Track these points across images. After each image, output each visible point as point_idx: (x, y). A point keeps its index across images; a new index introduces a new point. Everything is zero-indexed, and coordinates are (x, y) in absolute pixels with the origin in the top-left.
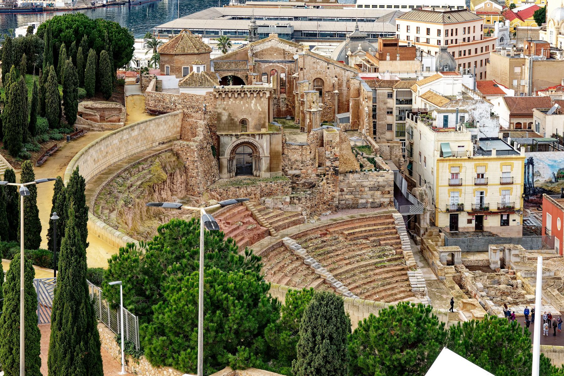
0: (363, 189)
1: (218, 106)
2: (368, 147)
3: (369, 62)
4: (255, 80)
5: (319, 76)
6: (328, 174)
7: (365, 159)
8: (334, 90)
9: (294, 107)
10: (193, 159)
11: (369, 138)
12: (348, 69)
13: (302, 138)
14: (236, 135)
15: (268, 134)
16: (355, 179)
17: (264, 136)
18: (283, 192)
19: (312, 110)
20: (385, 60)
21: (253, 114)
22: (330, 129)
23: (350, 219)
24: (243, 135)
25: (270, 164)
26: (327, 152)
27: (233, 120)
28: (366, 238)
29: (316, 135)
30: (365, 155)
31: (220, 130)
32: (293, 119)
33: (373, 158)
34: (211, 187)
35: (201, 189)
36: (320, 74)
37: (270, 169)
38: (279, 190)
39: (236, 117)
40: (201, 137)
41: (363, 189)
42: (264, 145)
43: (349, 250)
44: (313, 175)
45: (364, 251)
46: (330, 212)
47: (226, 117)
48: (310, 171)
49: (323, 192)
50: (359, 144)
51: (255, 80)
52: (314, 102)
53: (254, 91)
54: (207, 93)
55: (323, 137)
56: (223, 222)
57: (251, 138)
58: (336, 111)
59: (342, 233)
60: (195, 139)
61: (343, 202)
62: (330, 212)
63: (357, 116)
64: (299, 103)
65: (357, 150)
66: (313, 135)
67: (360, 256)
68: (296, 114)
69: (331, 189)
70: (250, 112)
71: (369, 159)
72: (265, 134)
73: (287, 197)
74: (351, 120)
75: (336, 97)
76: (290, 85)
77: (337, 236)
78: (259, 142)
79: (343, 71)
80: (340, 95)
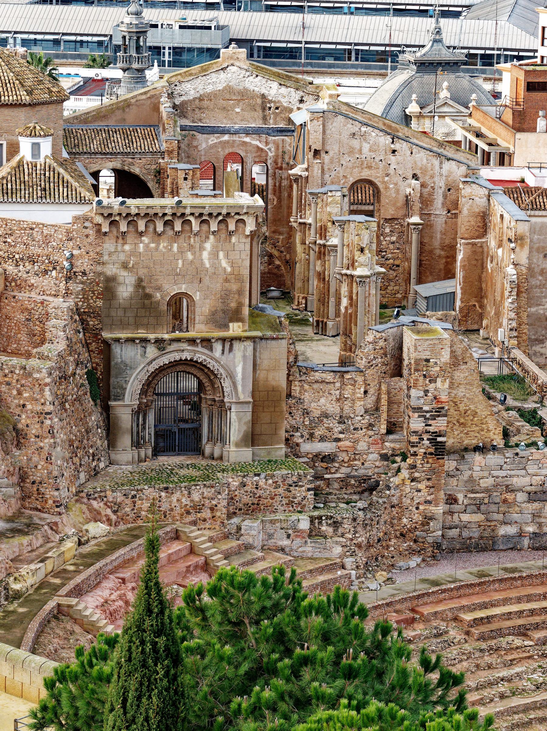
0: (510, 497)
1: (106, 258)
2: (516, 380)
3: (479, 135)
4: (189, 182)
5: (366, 174)
6: (415, 454)
7: (513, 413)
8: (408, 215)
9: (290, 264)
10: (39, 408)
11: (518, 354)
12: (450, 155)
13: (324, 352)
14: (159, 342)
15: (248, 338)
16: (488, 468)
17: (237, 345)
18: (290, 503)
19: (359, 272)
20: (533, 130)
21: (206, 280)
22: (420, 326)
23: (477, 581)
24: (178, 340)
25: (254, 421)
26: (414, 393)
27: (148, 296)
28: (523, 632)
29: (381, 343)
30: (510, 402)
31: (111, 328)
32: (286, 296)
33: (535, 411)
34: (89, 488)
35: (64, 493)
36: (370, 167)
37: (252, 438)
38: (278, 498)
39: (159, 288)
40: (61, 346)
41: (510, 497)
42: (236, 368)
43: (477, 666)
44: (371, 457)
45: (518, 669)
46: (419, 560)
47: (131, 289)
48: (362, 446)
49: (399, 505)
50: (490, 370)
51: (189, 182)
52: (362, 250)
53: (210, 215)
54: (76, 219)
55: (400, 348)
56: (130, 585)
57: (200, 349)
58: (413, 275)
59: (456, 619)
60: (45, 349)
61: (454, 533)
62: (419, 560)
63: (478, 289)
64: (308, 250)
65: (487, 388)
66: (375, 342)
67: (509, 680)
68: (298, 284)
69: (424, 495)
70: (198, 275)
71: (522, 412)
72: (239, 339)
73: (301, 517)
74: (458, 303)
75: (414, 237)
76: (280, 199)
77: (443, 626)
78: (224, 360)
79: (436, 162)
80: (425, 229)
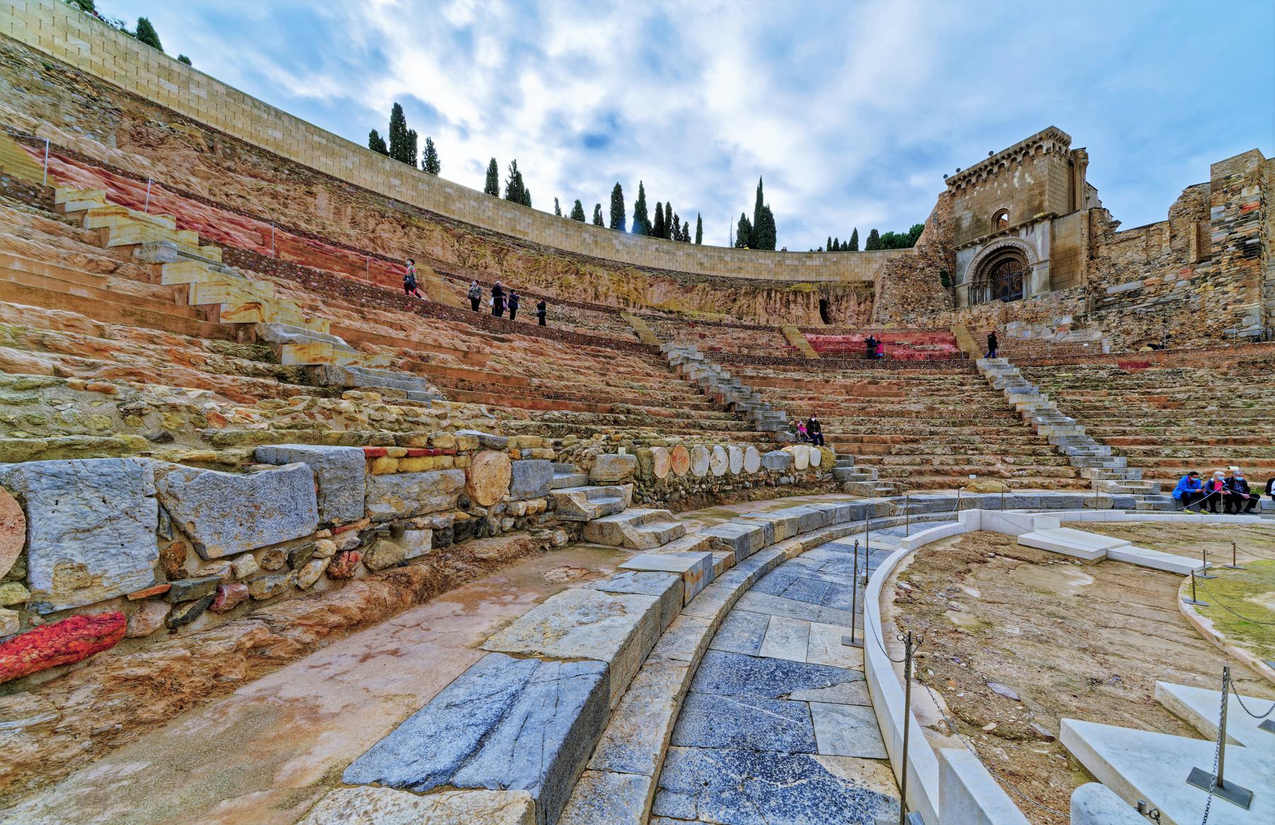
21: (1017, 196)
27: (979, 220)
44: (1179, 284)
49: (1202, 309)
53: (1016, 152)
70: (1011, 195)
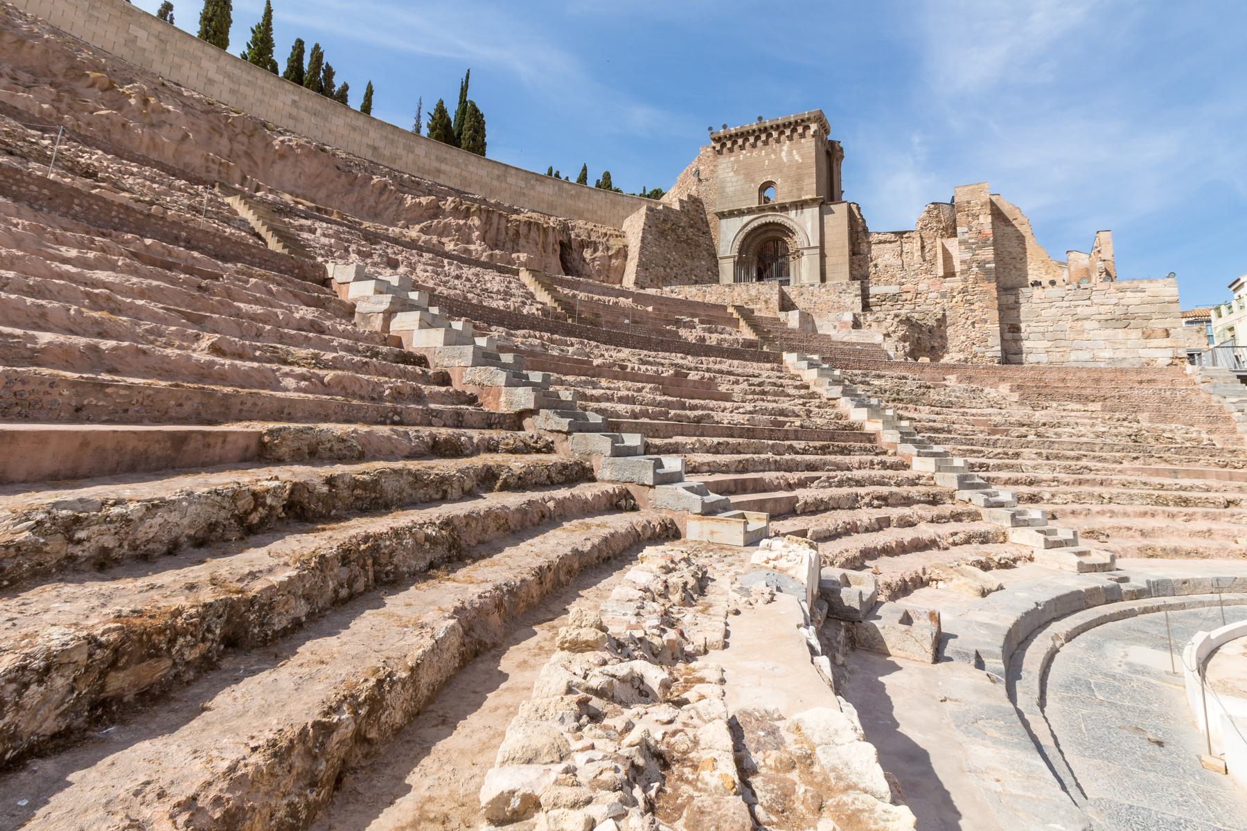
44: (931, 295)
